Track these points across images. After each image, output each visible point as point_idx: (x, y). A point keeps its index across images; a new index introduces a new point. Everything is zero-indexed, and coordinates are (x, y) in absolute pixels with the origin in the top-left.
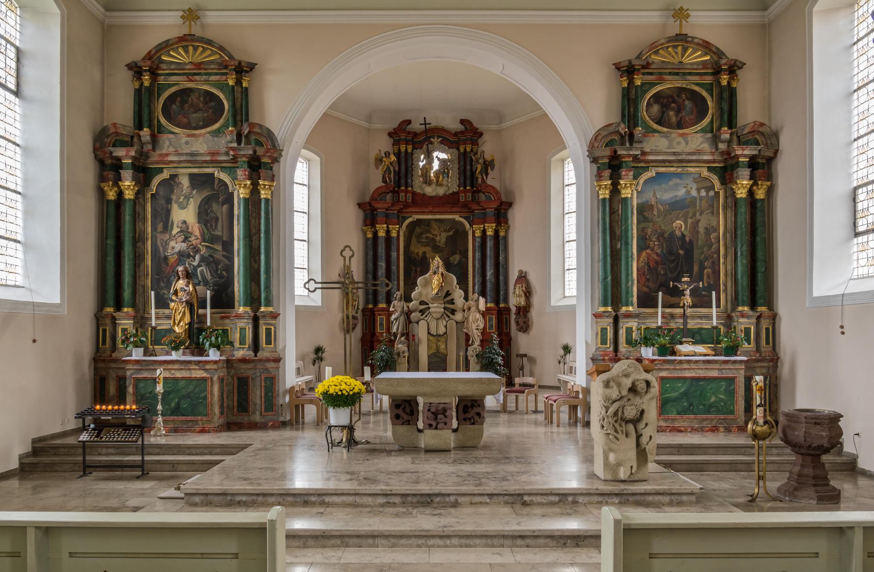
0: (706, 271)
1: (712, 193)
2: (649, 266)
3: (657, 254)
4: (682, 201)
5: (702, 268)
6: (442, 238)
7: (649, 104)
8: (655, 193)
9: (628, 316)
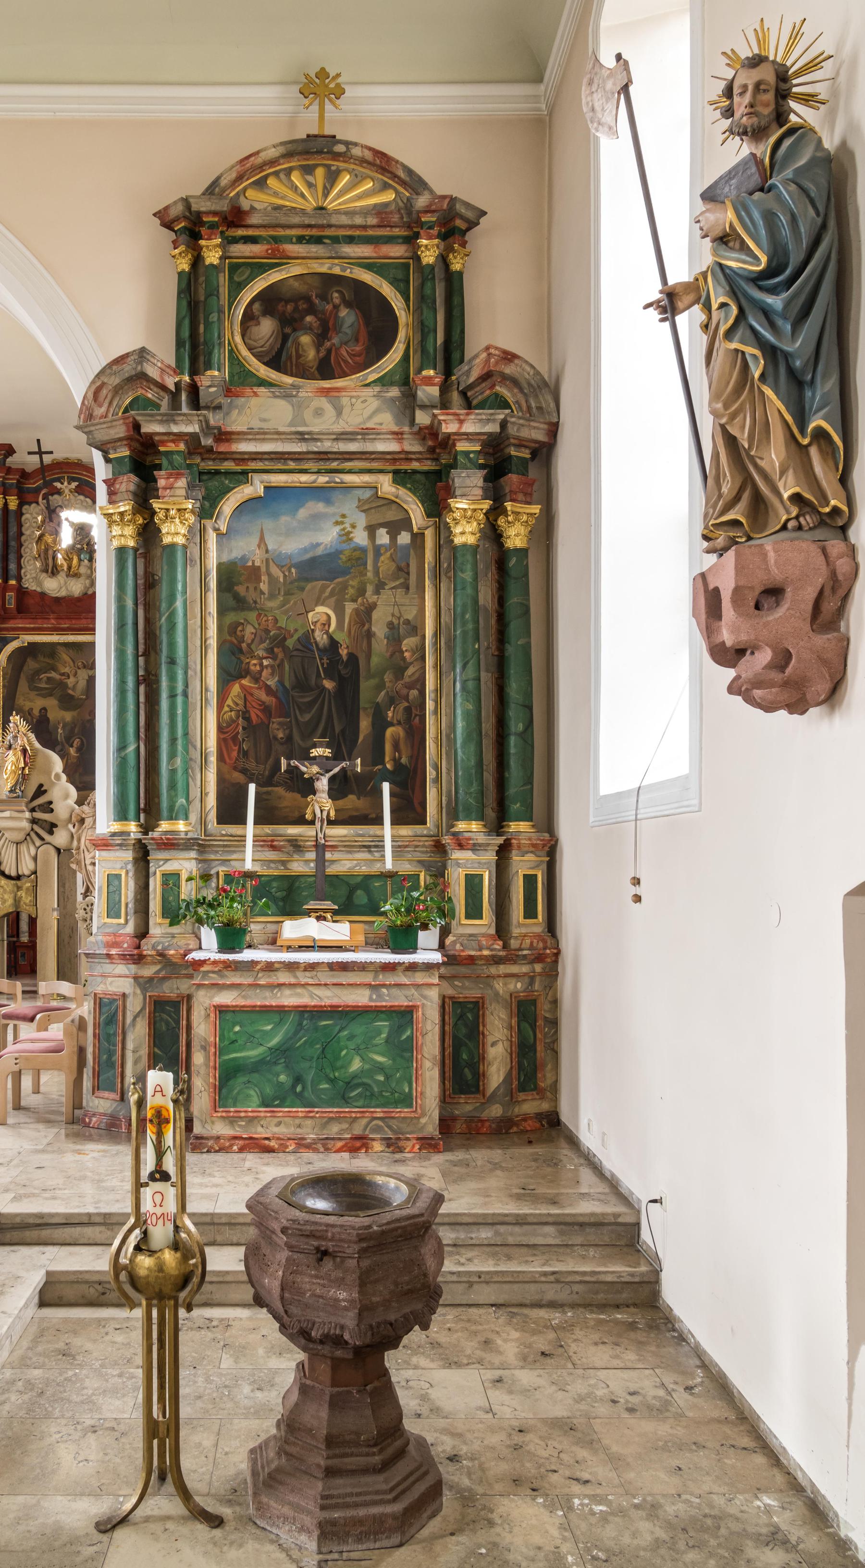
0: (390, 731)
1: (404, 538)
2: (247, 719)
3: (269, 690)
4: (333, 555)
5: (380, 724)
7: (249, 318)
8: (262, 539)
9: (170, 844)
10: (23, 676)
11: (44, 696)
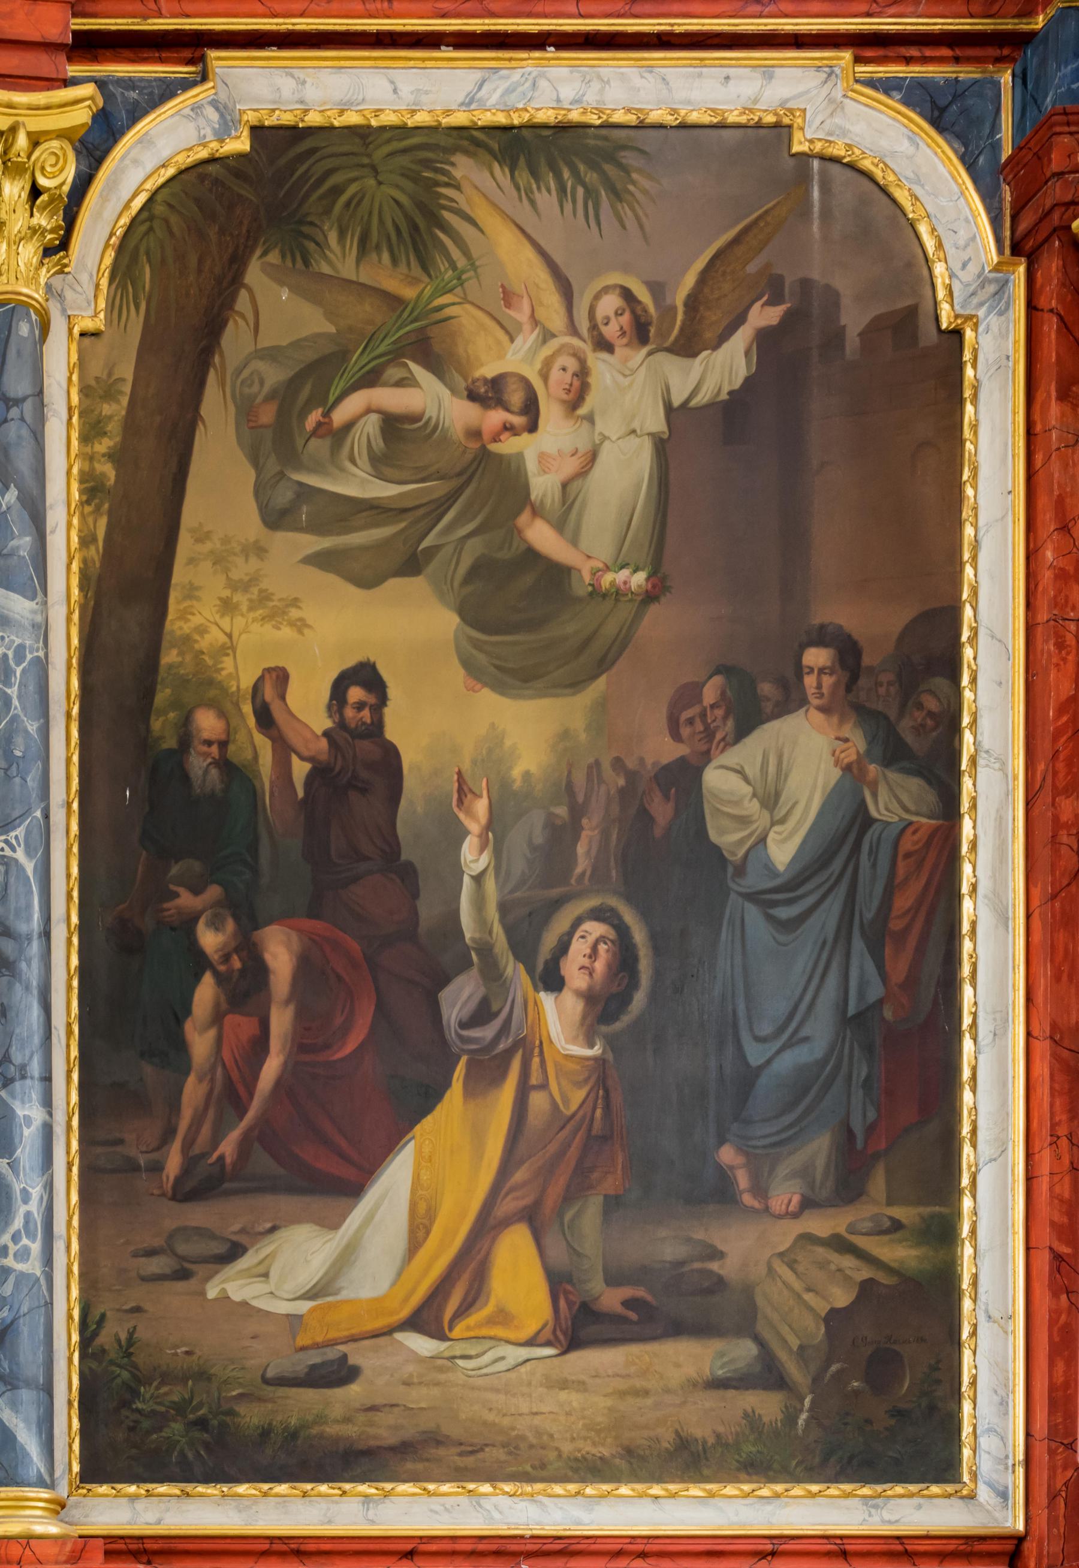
6: (600, 452)
10: (216, 408)
11: (366, 573)
